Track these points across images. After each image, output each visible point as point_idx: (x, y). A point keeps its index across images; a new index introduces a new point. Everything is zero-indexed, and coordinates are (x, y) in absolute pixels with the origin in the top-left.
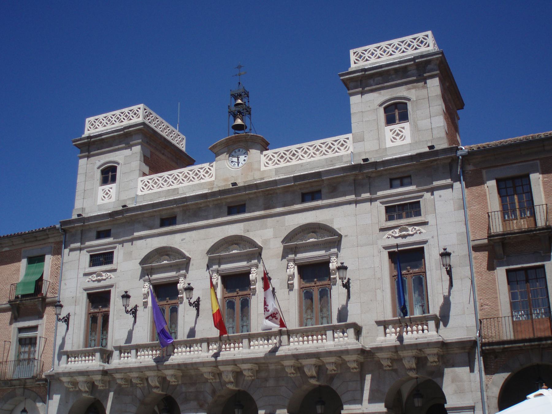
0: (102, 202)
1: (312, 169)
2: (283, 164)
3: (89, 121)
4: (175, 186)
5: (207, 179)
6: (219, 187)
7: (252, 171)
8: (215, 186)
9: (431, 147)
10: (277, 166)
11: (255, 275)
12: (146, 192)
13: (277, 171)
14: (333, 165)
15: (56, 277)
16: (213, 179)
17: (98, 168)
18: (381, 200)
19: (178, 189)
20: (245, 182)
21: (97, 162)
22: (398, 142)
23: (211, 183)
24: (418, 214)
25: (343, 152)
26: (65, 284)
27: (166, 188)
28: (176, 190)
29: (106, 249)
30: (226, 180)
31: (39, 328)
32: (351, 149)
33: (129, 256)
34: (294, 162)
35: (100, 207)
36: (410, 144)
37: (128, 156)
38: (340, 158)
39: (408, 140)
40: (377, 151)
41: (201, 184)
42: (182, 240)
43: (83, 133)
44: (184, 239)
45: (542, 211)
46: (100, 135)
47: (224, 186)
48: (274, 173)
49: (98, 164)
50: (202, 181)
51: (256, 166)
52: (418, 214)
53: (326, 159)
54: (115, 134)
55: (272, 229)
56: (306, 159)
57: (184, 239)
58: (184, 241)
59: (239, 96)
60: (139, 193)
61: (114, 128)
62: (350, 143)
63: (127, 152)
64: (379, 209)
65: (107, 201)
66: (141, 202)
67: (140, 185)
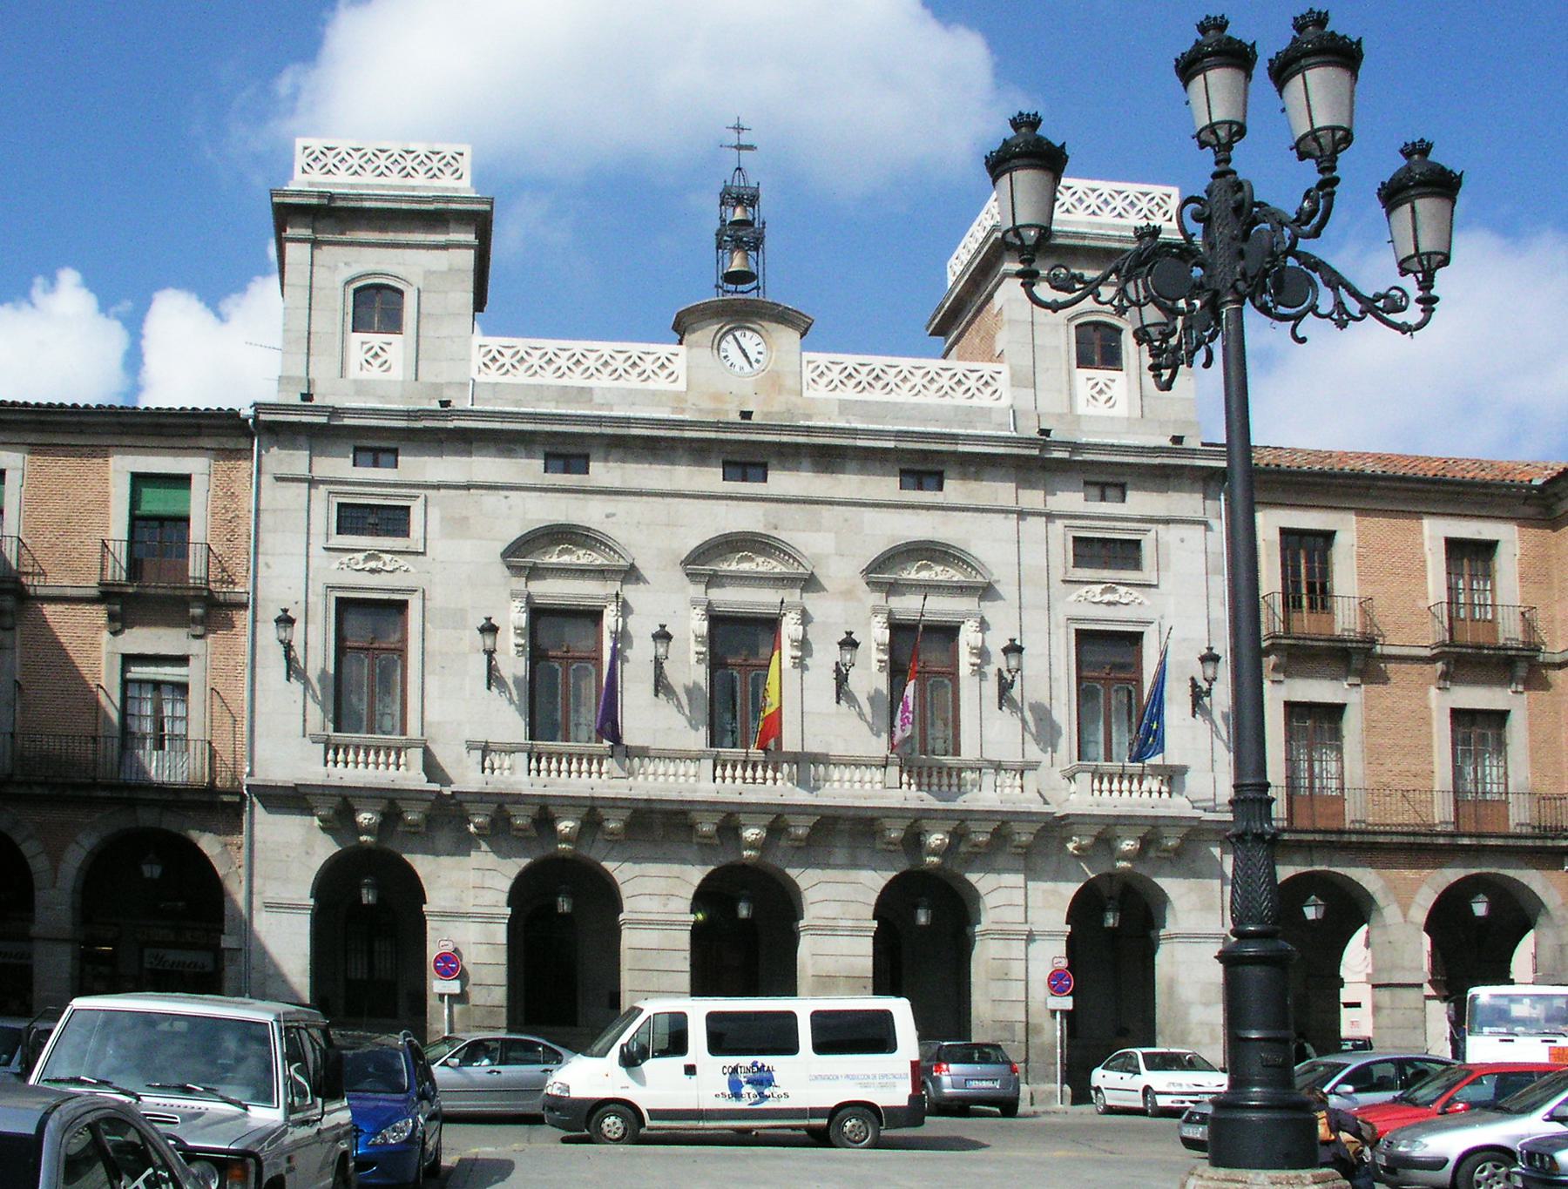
0: (364, 375)
1: (924, 421)
2: (849, 393)
3: (306, 148)
4: (576, 380)
5: (660, 383)
6: (700, 411)
7: (780, 393)
8: (689, 404)
9: (1177, 440)
10: (838, 394)
11: (790, 628)
12: (493, 376)
13: (845, 407)
14: (970, 424)
15: (228, 540)
16: (681, 386)
17: (348, 283)
18: (1067, 522)
19: (591, 389)
20: (766, 415)
21: (341, 265)
22: (1100, 409)
23: (679, 398)
24: (1136, 565)
25: (984, 400)
26: (267, 565)
27: (548, 378)
28: (584, 393)
29: (386, 496)
30: (717, 397)
31: (192, 661)
32: (1005, 402)
33: (458, 526)
34: (876, 395)
35: (361, 388)
36: (1128, 419)
37: (434, 272)
38: (985, 412)
39: (1121, 410)
40: (1061, 416)
41: (654, 393)
42: (607, 516)
43: (289, 174)
44: (614, 515)
45: (1346, 606)
46: (360, 197)
47: (715, 411)
48: (837, 409)
49: (348, 273)
50: (651, 385)
51: (790, 382)
52: (1136, 565)
53: (957, 408)
54: (405, 206)
55: (833, 535)
56: (903, 396)
57: (614, 515)
58: (613, 519)
59: (739, 201)
60: (474, 374)
61: (383, 187)
62: (1003, 381)
63: (439, 259)
64: (1060, 537)
65: (374, 373)
66: (487, 401)
67: (477, 358)
